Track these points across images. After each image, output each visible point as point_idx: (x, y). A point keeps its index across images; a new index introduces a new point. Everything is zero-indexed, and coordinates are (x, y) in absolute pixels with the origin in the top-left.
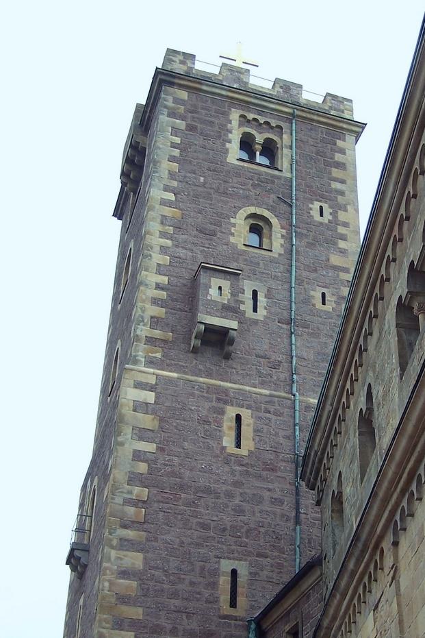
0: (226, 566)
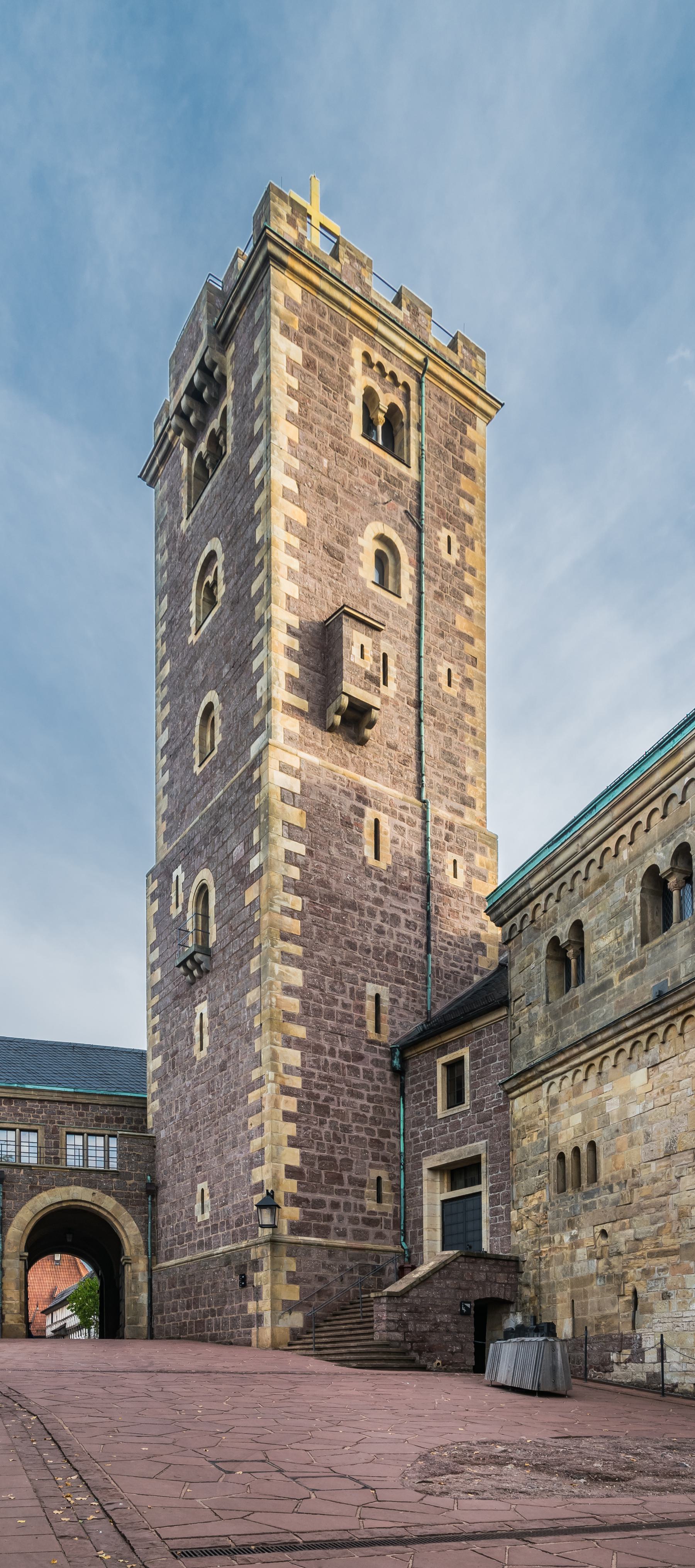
0: (371, 989)
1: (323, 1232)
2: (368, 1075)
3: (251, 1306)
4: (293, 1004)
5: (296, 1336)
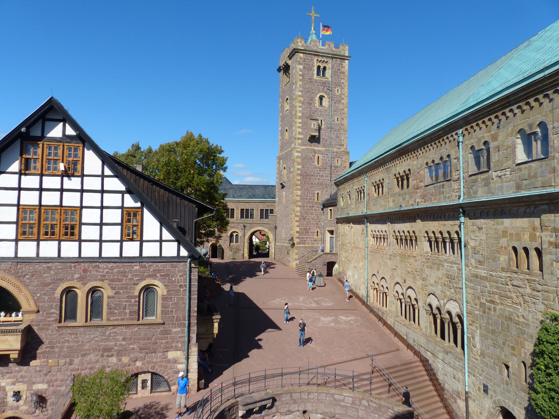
0: (316, 192)
2: (315, 210)
4: (298, 198)
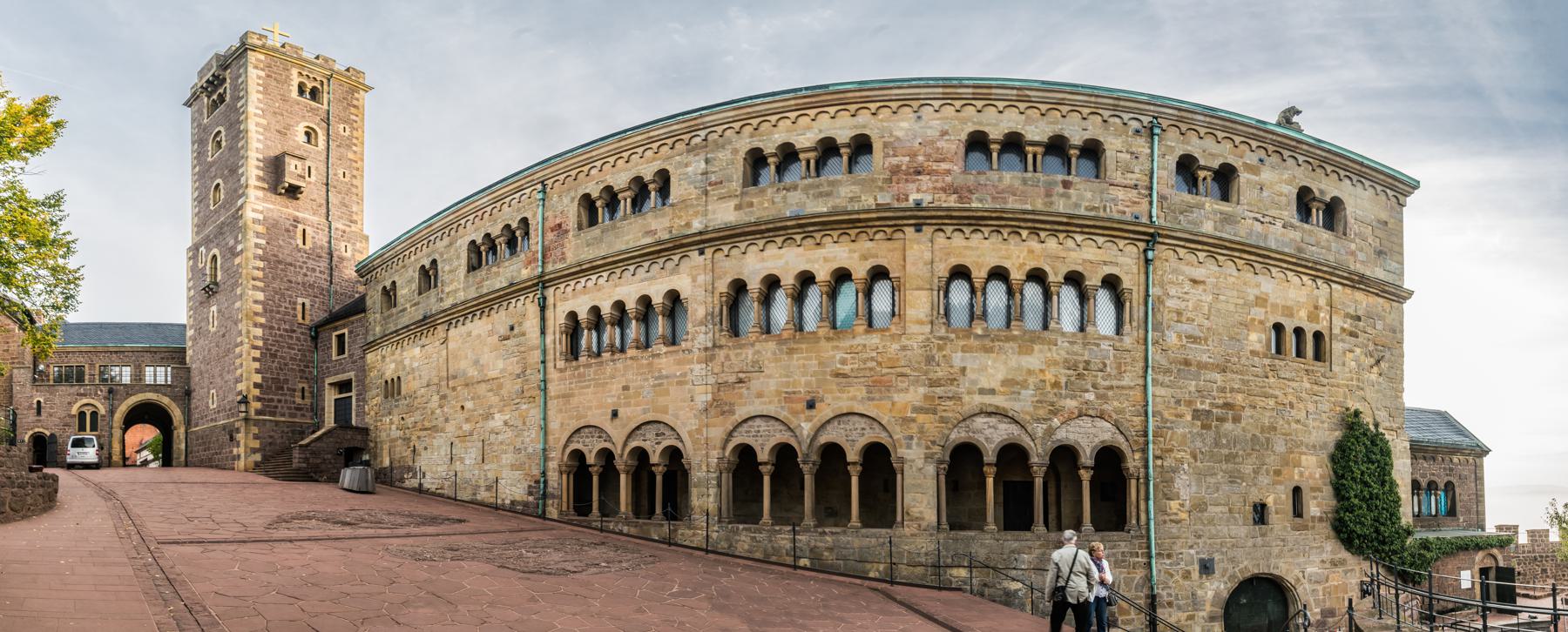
1: (273, 414)
2: (298, 339)
3: (235, 451)
5: (257, 465)
